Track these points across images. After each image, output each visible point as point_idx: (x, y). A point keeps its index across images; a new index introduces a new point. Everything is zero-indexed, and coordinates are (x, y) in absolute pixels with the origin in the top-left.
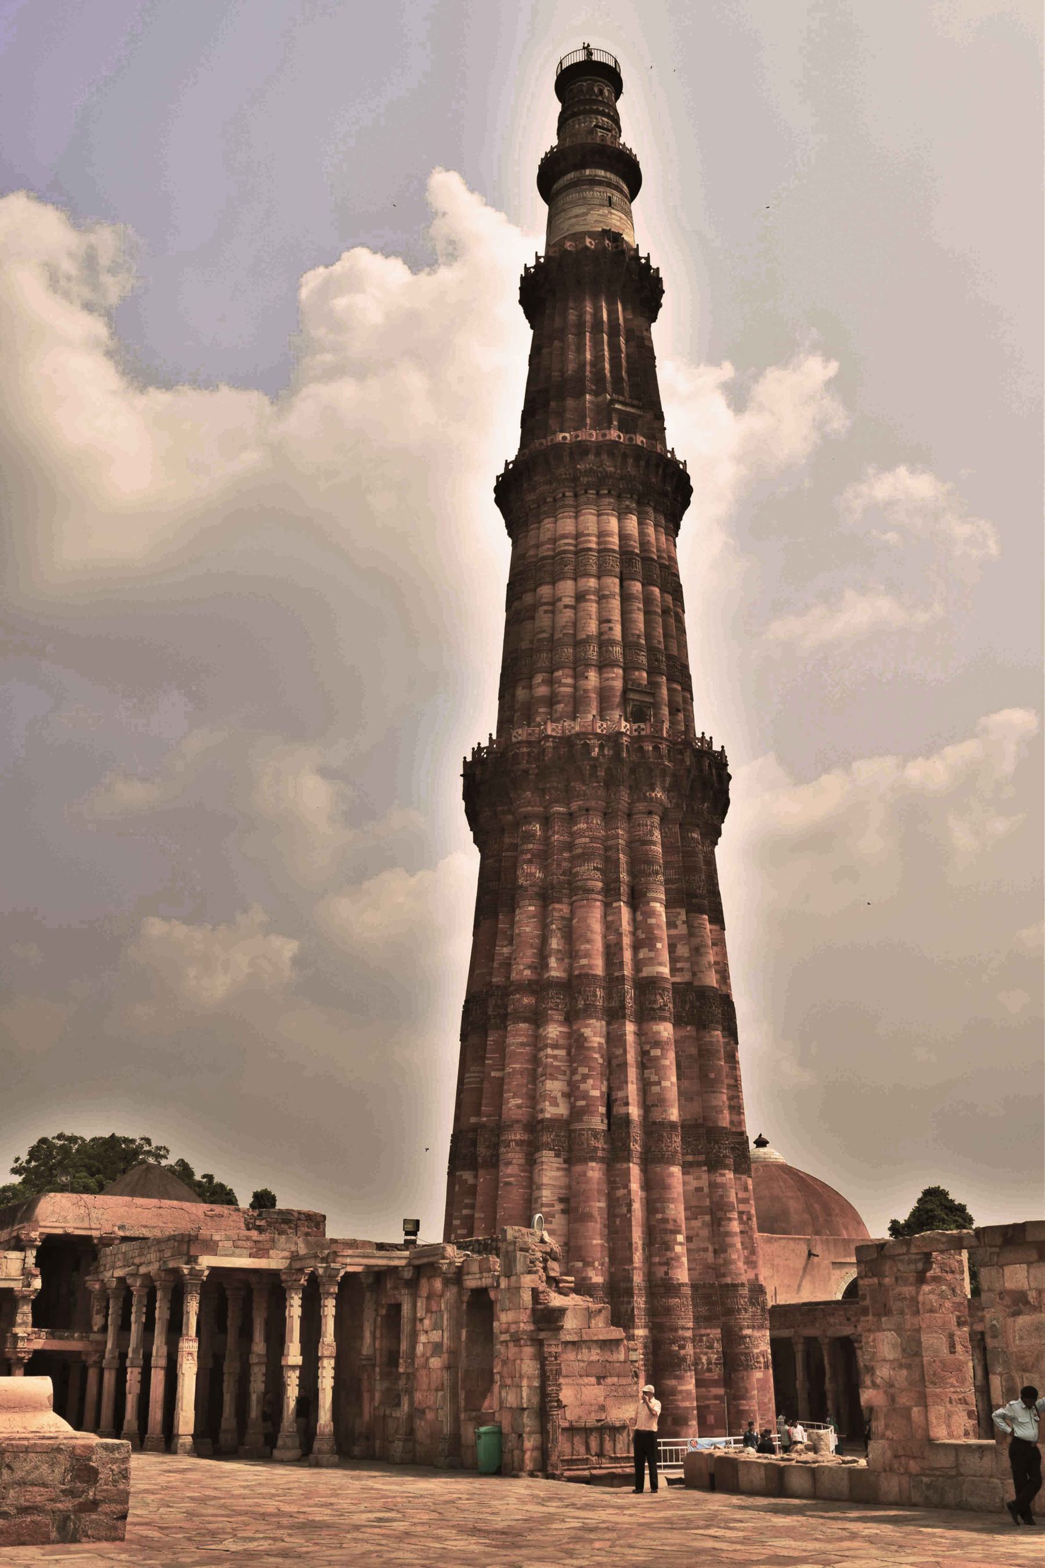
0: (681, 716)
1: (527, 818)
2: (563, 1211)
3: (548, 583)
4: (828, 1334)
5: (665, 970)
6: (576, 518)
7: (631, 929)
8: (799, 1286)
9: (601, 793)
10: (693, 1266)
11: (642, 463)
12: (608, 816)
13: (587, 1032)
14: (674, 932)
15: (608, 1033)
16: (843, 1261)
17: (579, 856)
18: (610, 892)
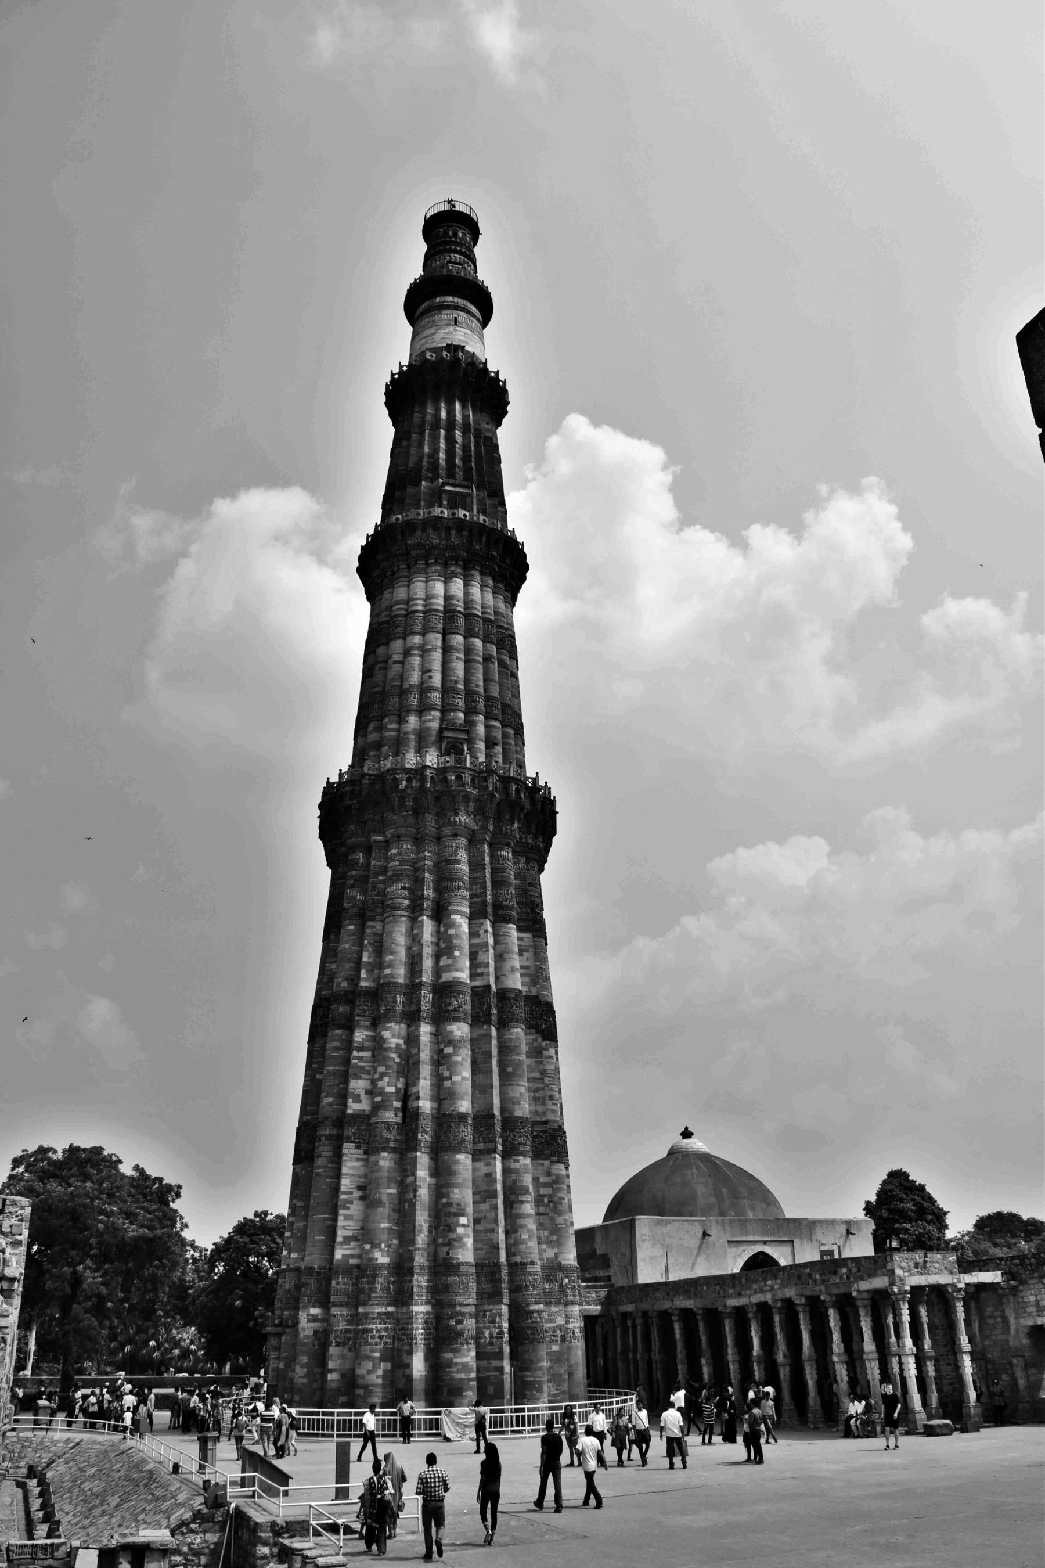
0: (499, 749)
1: (353, 849)
2: (362, 1198)
3: (383, 644)
4: (656, 1308)
5: (464, 976)
6: (408, 586)
7: (435, 940)
8: (694, 1264)
9: (411, 820)
10: (480, 1246)
11: (465, 533)
12: (418, 841)
13: (386, 1034)
14: (475, 941)
15: (408, 1035)
16: (740, 1239)
17: (390, 878)
18: (415, 910)
